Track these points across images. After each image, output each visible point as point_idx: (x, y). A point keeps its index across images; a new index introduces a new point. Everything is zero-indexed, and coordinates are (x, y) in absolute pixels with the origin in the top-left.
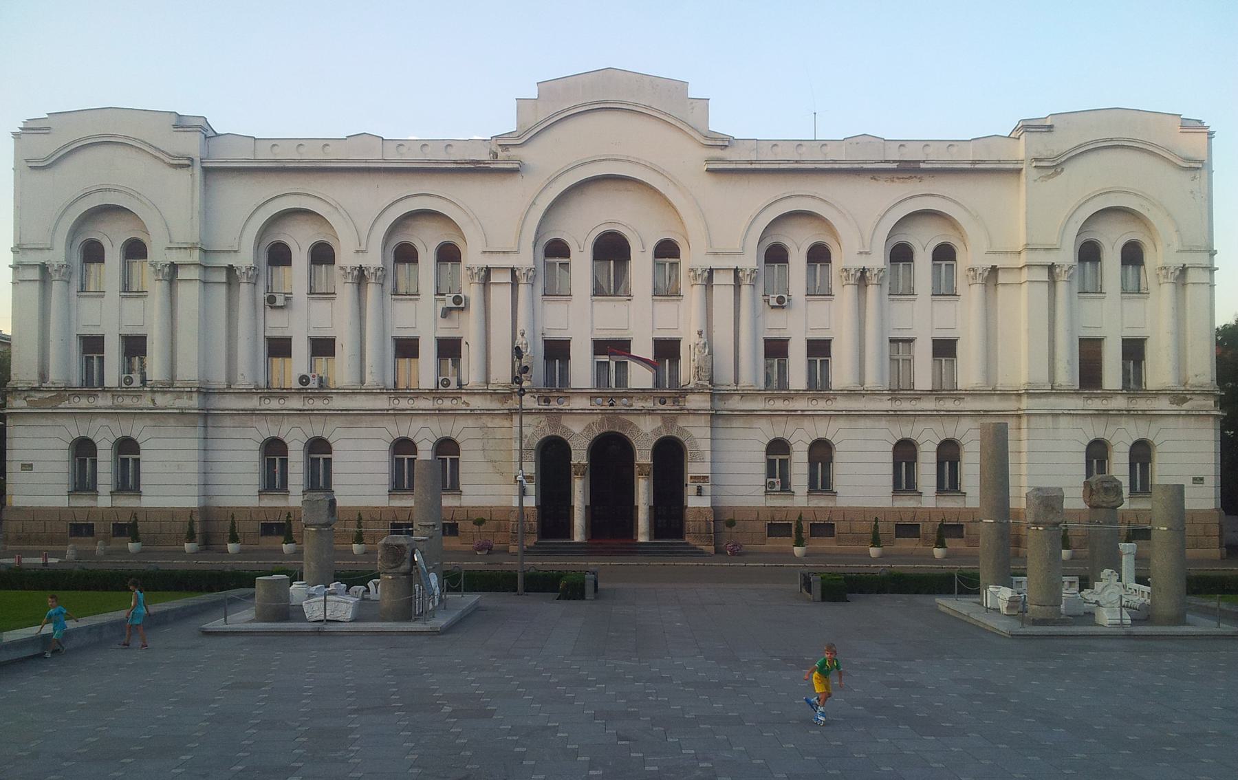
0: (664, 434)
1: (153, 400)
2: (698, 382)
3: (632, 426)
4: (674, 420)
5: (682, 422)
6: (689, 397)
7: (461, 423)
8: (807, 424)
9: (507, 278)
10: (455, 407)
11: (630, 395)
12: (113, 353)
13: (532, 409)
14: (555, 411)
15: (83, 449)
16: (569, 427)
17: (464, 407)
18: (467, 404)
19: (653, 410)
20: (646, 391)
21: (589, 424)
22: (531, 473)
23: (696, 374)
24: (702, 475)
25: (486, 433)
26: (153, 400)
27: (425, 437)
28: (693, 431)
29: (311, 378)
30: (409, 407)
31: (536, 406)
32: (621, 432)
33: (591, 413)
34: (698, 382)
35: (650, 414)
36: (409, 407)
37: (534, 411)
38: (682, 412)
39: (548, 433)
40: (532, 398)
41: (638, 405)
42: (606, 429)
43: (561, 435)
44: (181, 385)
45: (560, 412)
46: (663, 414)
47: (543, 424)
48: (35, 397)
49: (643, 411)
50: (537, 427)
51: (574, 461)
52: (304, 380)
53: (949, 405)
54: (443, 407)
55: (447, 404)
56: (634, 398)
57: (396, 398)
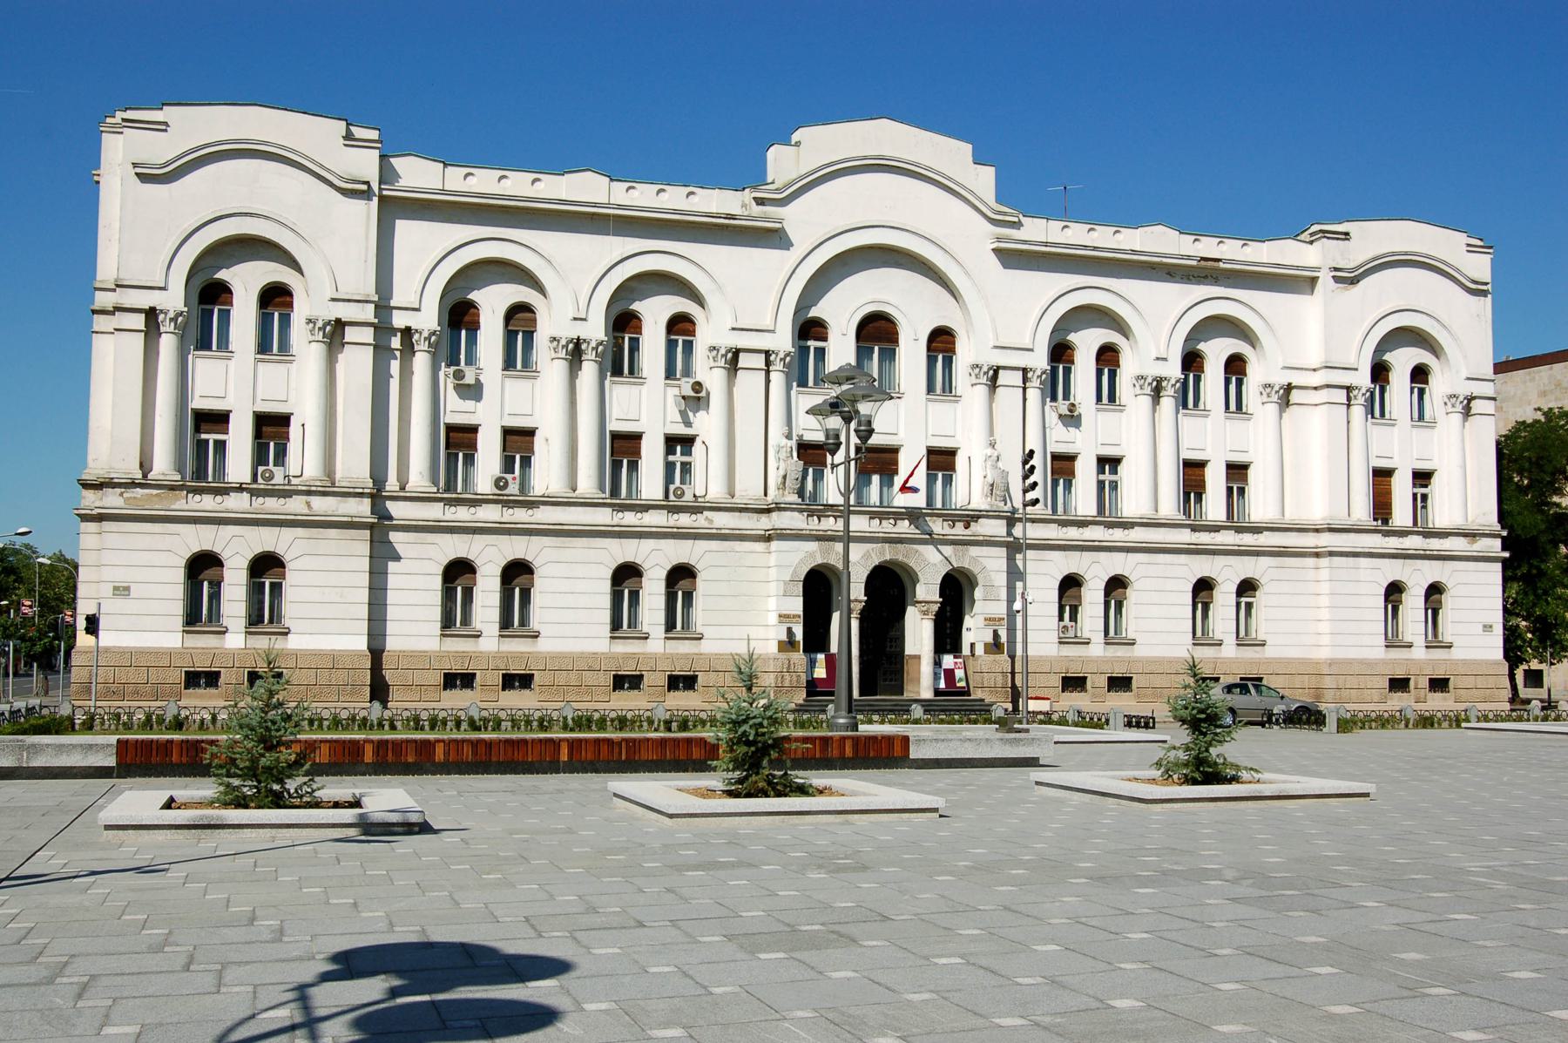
1: (308, 504)
8: (1103, 556)
9: (759, 361)
10: (695, 525)
12: (239, 439)
15: (203, 566)
18: (711, 521)
24: (997, 616)
26: (308, 504)
27: (656, 560)
29: (510, 481)
30: (638, 523)
44: (349, 485)
48: (137, 493)
52: (500, 484)
53: (1248, 539)
55: (684, 520)
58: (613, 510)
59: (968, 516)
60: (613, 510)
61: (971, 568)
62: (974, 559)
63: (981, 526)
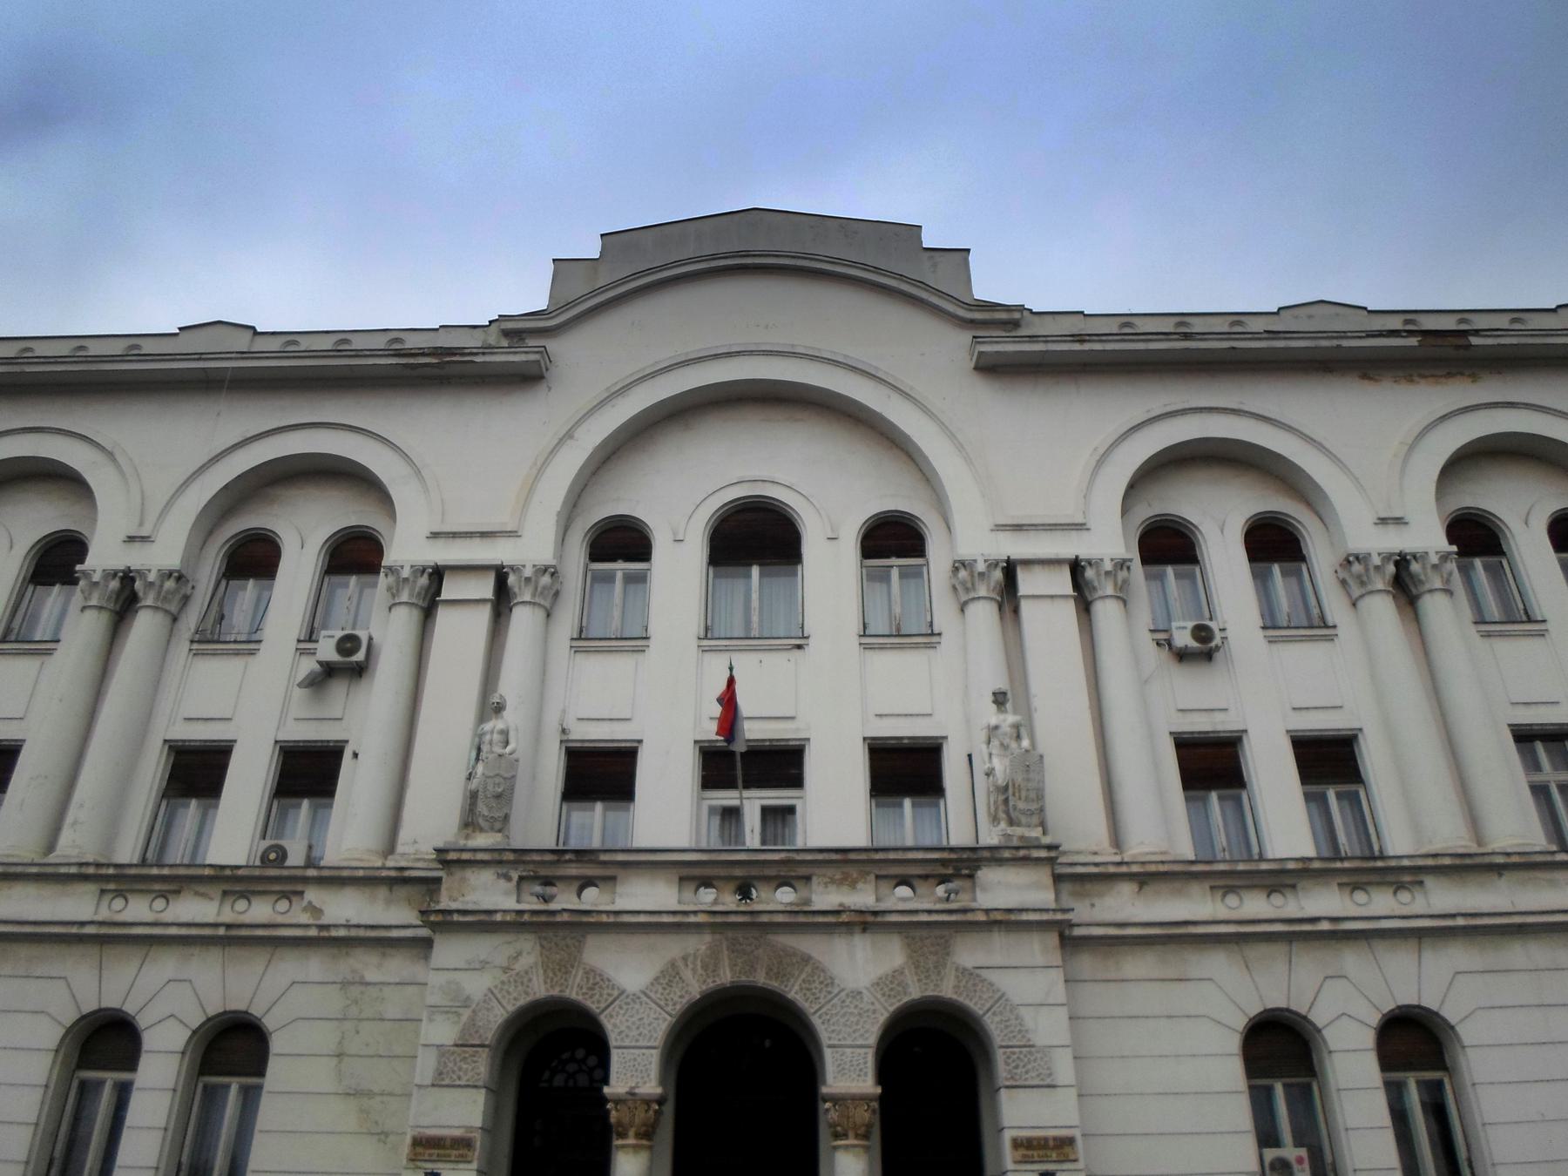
0: (915, 992)
2: (1010, 830)
3: (808, 969)
4: (945, 950)
5: (969, 953)
6: (987, 875)
7: (291, 967)
8: (1352, 960)
10: (280, 919)
11: (802, 871)
13: (496, 912)
14: (565, 917)
16: (610, 972)
17: (304, 918)
18: (315, 911)
19: (875, 913)
20: (853, 856)
21: (673, 964)
22: (469, 1129)
23: (1002, 808)
25: (356, 1002)
28: (1002, 980)
31: (510, 903)
32: (774, 985)
33: (674, 925)
34: (1010, 830)
35: (865, 927)
36: (148, 917)
37: (498, 917)
38: (970, 917)
39: (540, 989)
40: (502, 882)
41: (826, 897)
42: (726, 976)
43: (580, 998)
45: (584, 925)
46: (908, 928)
47: (522, 965)
49: (844, 918)
50: (506, 970)
51: (616, 1086)
54: (247, 918)
56: (815, 880)
57: (120, 893)
58: (103, 892)
59: (944, 863)
60: (103, 892)
61: (961, 999)
62: (970, 976)
63: (984, 890)
